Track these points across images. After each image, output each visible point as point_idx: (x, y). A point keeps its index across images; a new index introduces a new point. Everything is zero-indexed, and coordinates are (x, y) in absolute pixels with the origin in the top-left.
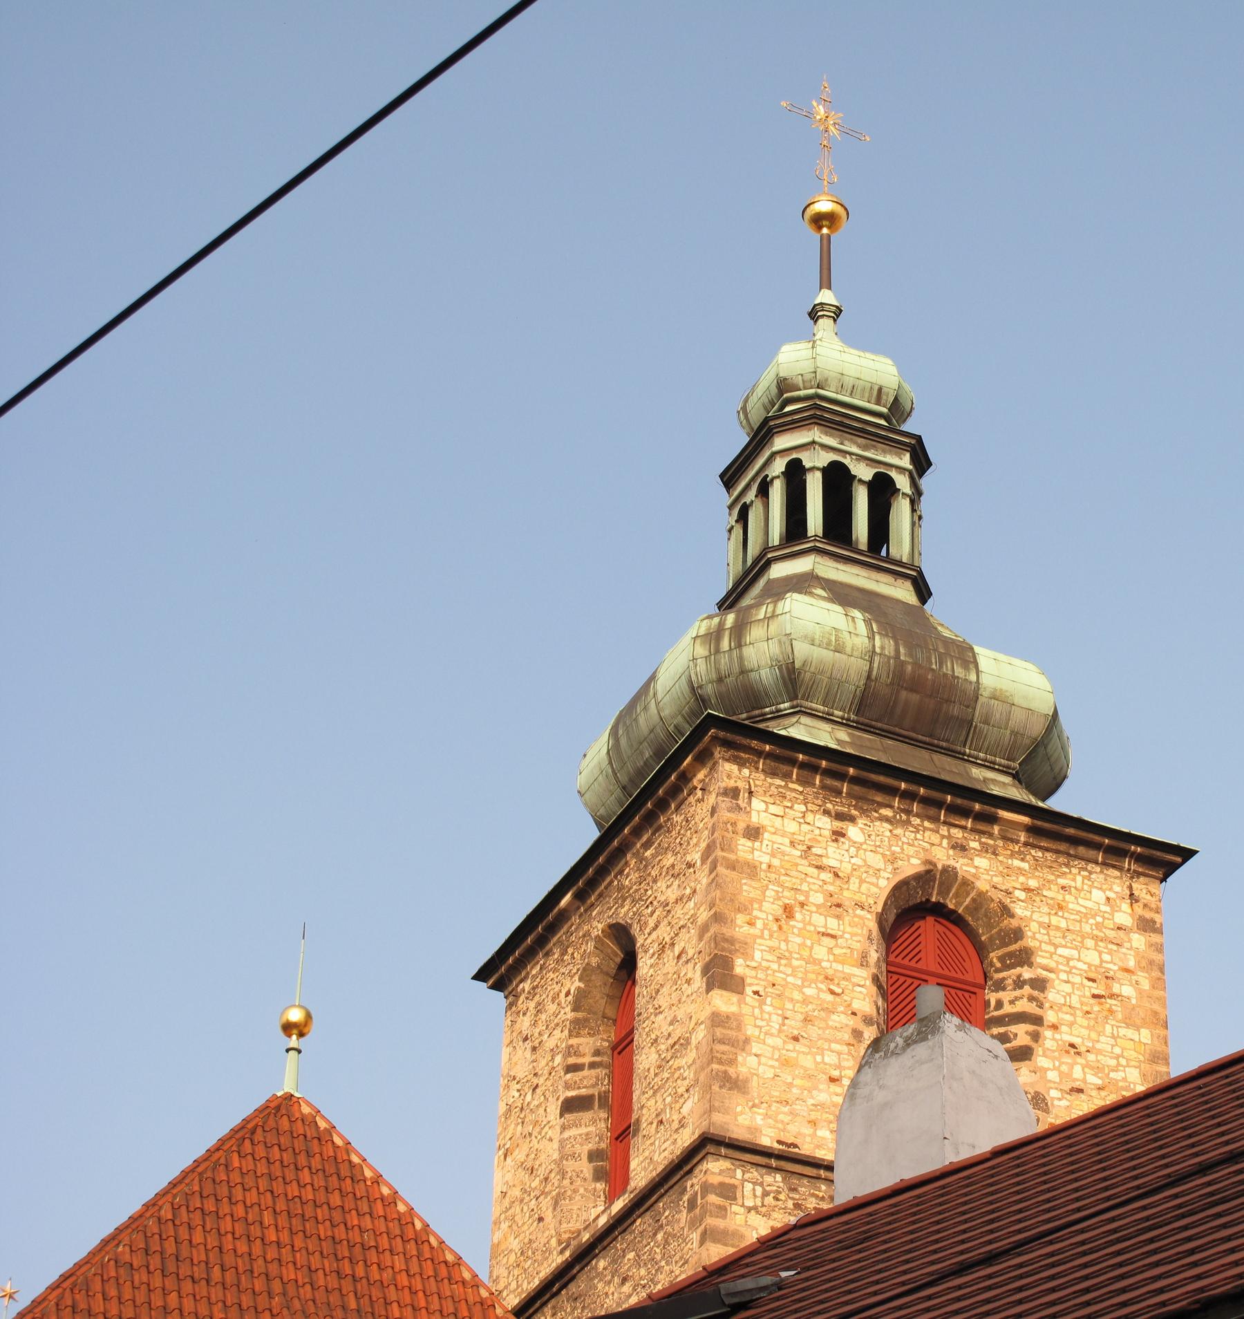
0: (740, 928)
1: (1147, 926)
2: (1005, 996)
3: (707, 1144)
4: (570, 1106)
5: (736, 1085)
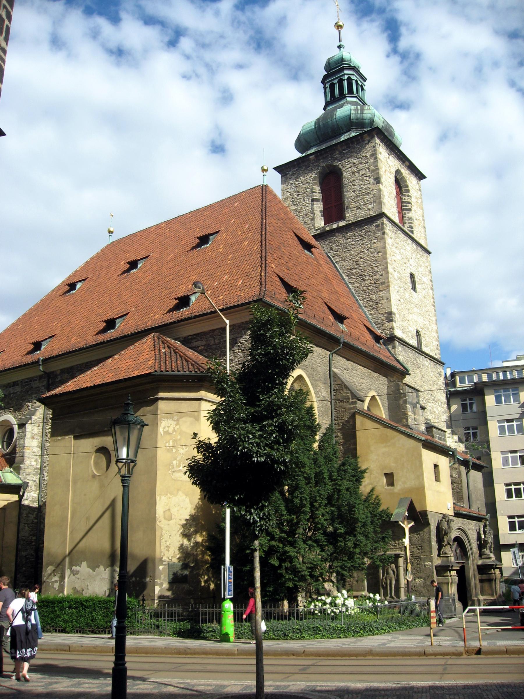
1: (420, 190)
2: (406, 198)
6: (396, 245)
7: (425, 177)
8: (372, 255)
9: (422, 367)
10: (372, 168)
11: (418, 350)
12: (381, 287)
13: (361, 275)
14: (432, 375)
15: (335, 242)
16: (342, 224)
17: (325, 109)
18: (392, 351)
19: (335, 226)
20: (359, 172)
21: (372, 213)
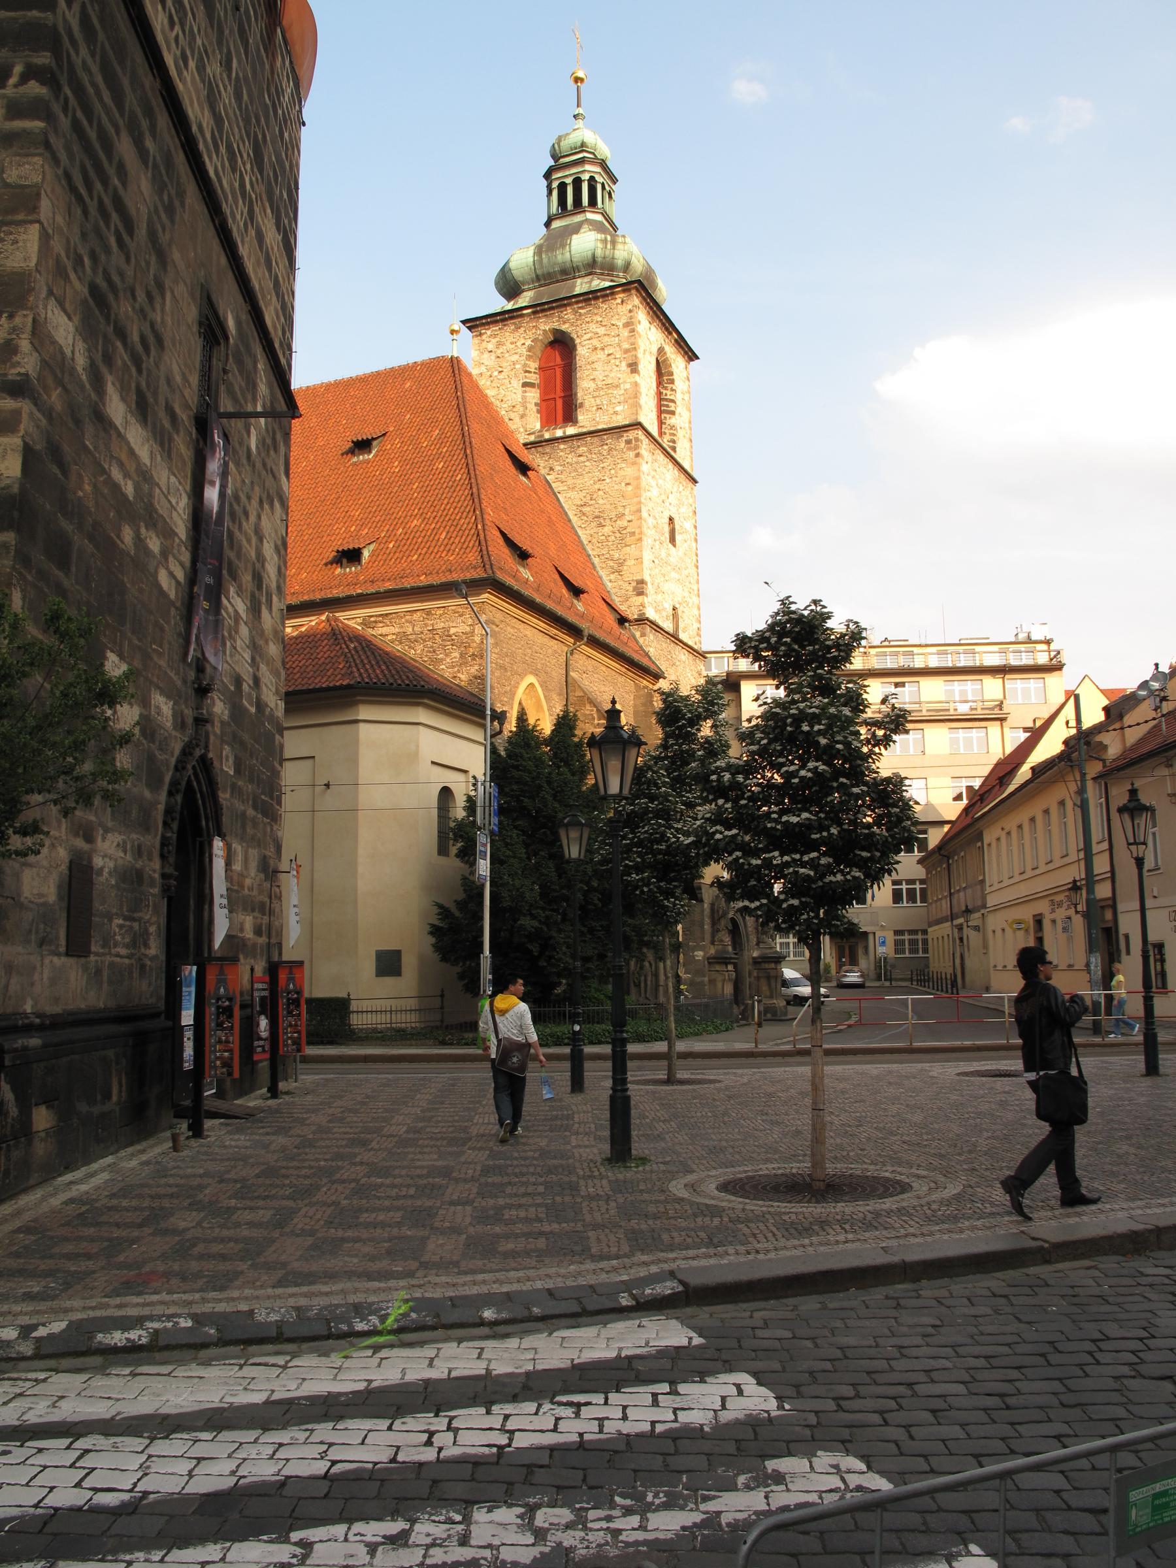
2: (669, 392)
4: (525, 385)
6: (653, 473)
7: (697, 358)
8: (616, 487)
10: (626, 346)
11: (674, 638)
12: (628, 540)
15: (558, 459)
16: (571, 430)
17: (548, 225)
18: (641, 641)
19: (559, 433)
20: (603, 349)
21: (621, 420)
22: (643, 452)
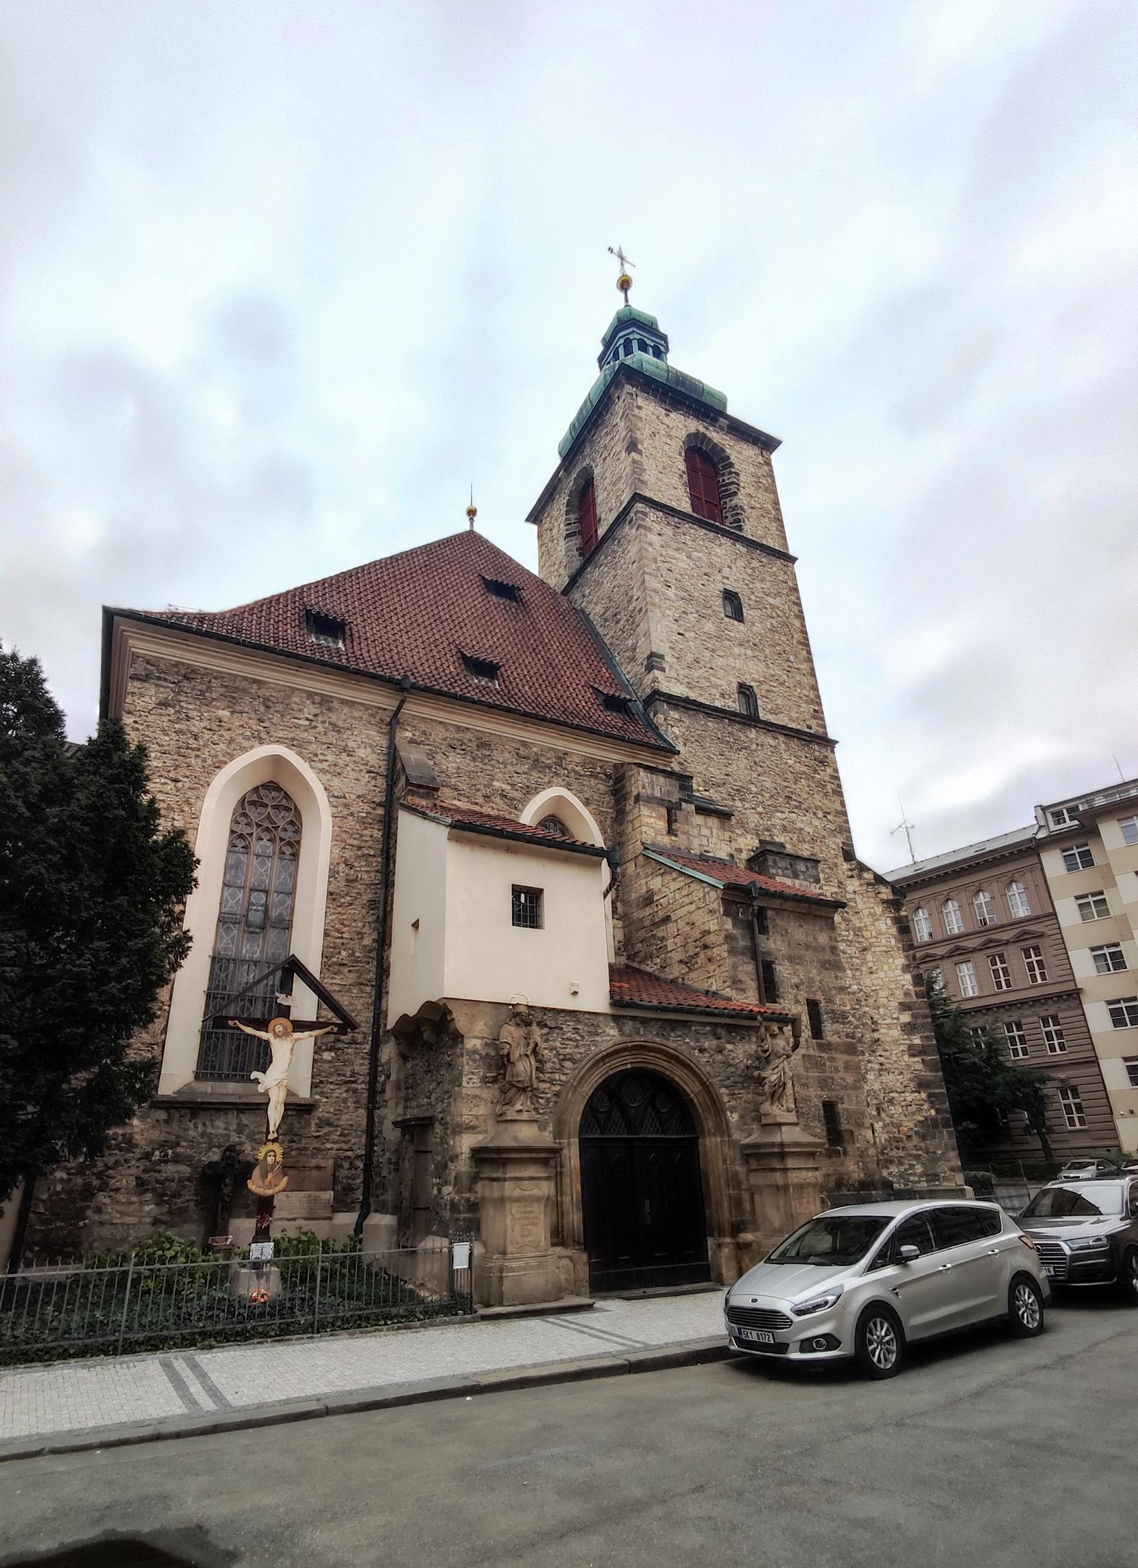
0: (638, 435)
2: (725, 478)
3: (637, 498)
5: (644, 483)
6: (675, 546)
7: (779, 443)
9: (754, 747)
13: (615, 615)
14: (791, 762)
22: (648, 522)
